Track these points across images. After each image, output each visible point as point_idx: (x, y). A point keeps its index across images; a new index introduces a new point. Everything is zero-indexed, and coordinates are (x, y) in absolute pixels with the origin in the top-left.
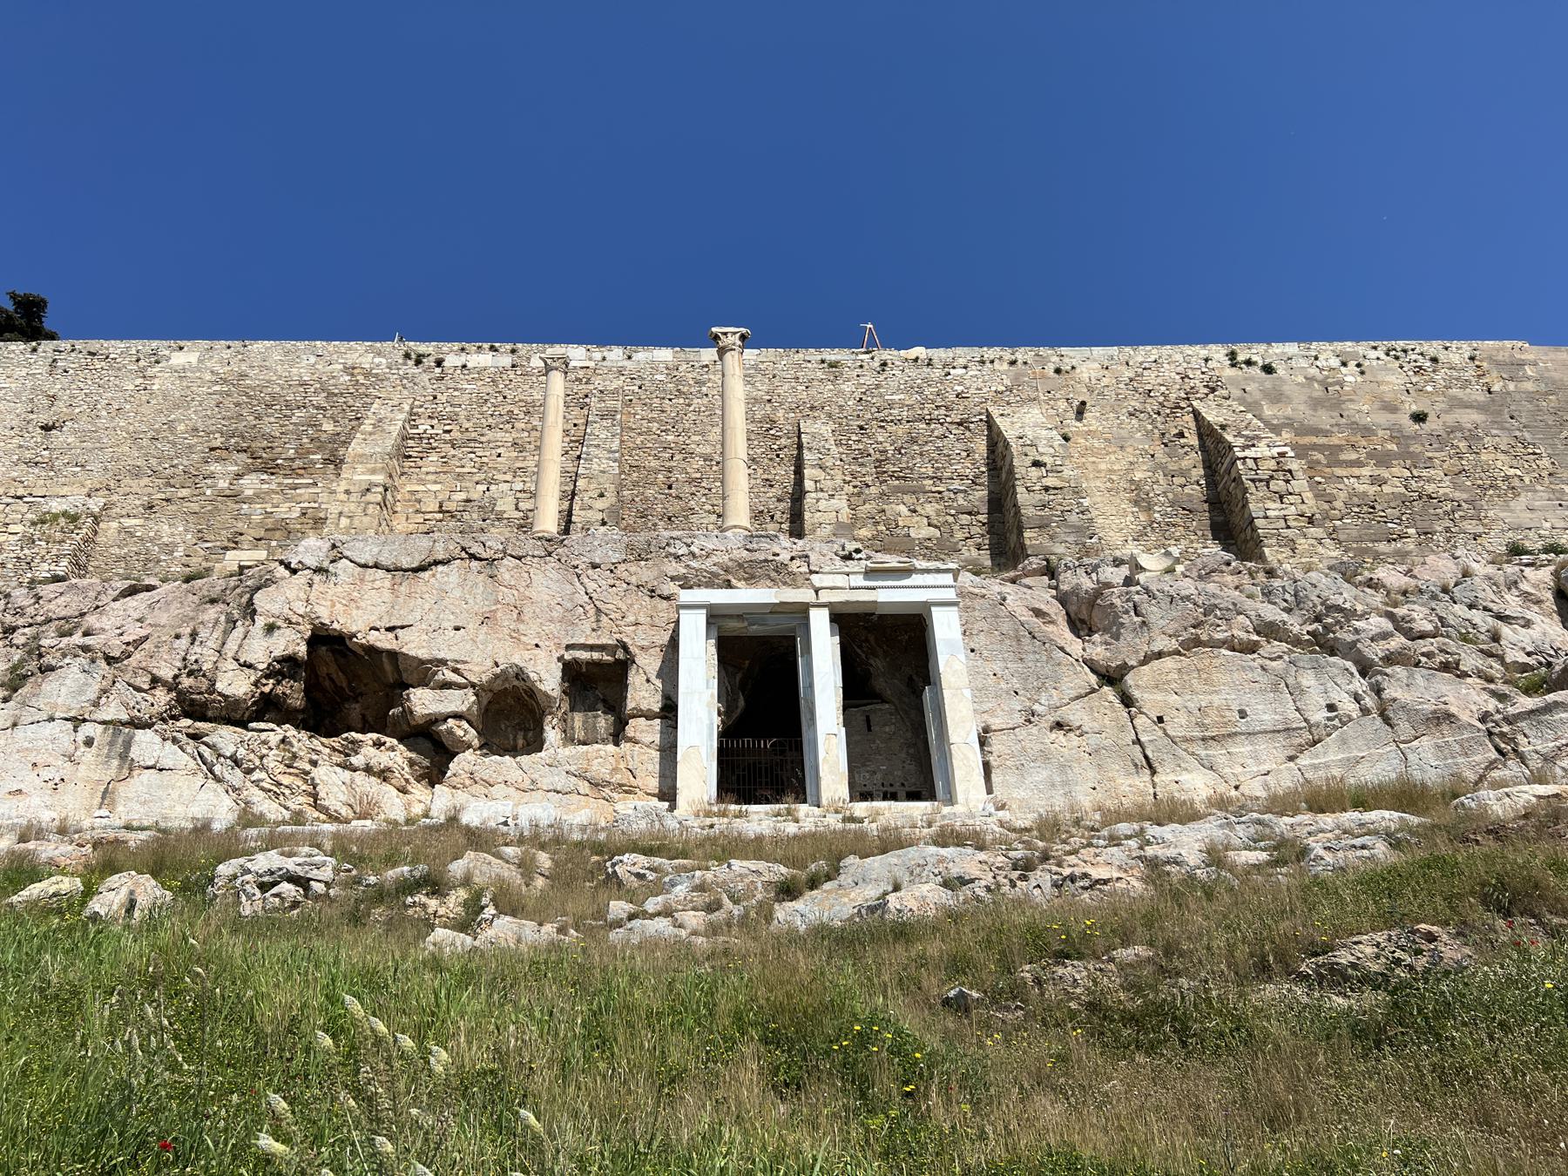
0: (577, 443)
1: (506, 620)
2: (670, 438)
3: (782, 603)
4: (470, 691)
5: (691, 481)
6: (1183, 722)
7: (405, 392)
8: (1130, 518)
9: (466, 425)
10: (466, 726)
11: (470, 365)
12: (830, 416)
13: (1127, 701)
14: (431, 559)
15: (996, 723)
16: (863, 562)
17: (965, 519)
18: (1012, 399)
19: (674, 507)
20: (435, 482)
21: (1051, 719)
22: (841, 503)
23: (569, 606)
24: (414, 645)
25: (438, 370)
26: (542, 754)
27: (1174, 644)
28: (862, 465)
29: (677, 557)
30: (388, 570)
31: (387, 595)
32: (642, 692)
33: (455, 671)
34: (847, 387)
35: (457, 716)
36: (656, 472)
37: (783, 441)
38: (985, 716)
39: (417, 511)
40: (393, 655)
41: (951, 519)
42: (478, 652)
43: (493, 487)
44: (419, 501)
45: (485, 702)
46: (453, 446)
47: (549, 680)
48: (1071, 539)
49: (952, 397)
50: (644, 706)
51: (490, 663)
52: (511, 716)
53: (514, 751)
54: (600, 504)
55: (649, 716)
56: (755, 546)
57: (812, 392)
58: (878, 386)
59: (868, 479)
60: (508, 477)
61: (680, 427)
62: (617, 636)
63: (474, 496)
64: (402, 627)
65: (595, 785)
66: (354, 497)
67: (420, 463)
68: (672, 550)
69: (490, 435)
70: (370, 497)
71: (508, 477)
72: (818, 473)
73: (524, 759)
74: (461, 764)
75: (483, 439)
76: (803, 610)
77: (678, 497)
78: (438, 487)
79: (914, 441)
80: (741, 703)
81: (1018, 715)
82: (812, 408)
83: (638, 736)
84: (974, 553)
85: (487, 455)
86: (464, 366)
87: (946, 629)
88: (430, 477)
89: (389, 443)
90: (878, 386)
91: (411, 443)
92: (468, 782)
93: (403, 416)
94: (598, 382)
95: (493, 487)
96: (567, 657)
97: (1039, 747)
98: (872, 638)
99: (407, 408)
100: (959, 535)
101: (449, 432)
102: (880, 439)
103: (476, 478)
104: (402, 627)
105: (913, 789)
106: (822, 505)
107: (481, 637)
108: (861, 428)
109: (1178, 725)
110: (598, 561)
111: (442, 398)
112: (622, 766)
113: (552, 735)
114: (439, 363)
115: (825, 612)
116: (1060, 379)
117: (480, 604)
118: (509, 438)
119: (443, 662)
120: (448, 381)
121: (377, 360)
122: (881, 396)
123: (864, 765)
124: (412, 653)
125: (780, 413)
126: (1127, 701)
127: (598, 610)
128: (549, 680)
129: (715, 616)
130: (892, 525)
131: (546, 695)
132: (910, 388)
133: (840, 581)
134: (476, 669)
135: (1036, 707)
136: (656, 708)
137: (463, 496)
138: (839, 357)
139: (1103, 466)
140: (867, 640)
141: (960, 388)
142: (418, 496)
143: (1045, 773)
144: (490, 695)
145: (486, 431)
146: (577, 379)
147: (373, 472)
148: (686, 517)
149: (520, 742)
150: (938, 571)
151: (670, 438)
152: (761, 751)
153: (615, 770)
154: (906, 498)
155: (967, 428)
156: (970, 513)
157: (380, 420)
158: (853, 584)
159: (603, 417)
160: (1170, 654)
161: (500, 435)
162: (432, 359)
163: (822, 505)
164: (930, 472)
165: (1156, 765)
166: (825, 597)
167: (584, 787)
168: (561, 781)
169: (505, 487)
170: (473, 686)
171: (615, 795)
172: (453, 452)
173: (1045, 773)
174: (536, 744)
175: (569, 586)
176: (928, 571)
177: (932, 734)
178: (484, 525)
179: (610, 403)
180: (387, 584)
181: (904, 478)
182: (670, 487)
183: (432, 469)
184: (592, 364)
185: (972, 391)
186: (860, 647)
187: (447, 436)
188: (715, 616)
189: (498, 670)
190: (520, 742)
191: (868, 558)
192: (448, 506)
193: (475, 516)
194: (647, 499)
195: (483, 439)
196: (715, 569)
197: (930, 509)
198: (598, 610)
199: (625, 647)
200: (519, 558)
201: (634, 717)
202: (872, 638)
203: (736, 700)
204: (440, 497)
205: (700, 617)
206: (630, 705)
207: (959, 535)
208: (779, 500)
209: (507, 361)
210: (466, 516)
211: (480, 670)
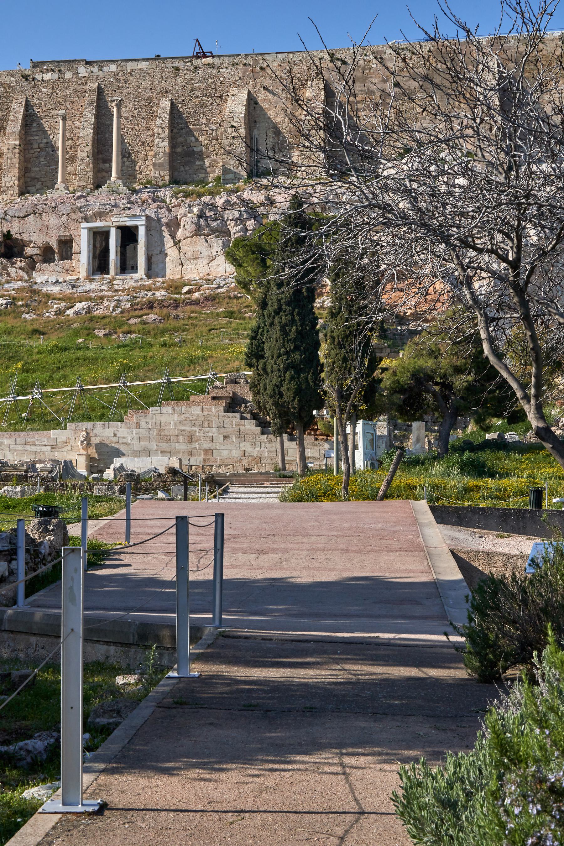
1: (45, 230)
13: (180, 249)
24: (25, 237)
47: (54, 245)
52: (47, 254)
54: (87, 149)
65: (67, 270)
66: (10, 151)
88: (35, 133)
90: (192, 79)
102: (189, 106)
108: (183, 101)
109: (189, 255)
117: (38, 225)
119: (32, 242)
126: (180, 249)
128: (54, 245)
129: (90, 229)
132: (205, 79)
138: (179, 65)
146: (82, 83)
152: (100, 265)
167: (64, 271)
168: (59, 270)
184: (86, 75)
207: (211, 149)
209: (56, 76)
211: (39, 243)
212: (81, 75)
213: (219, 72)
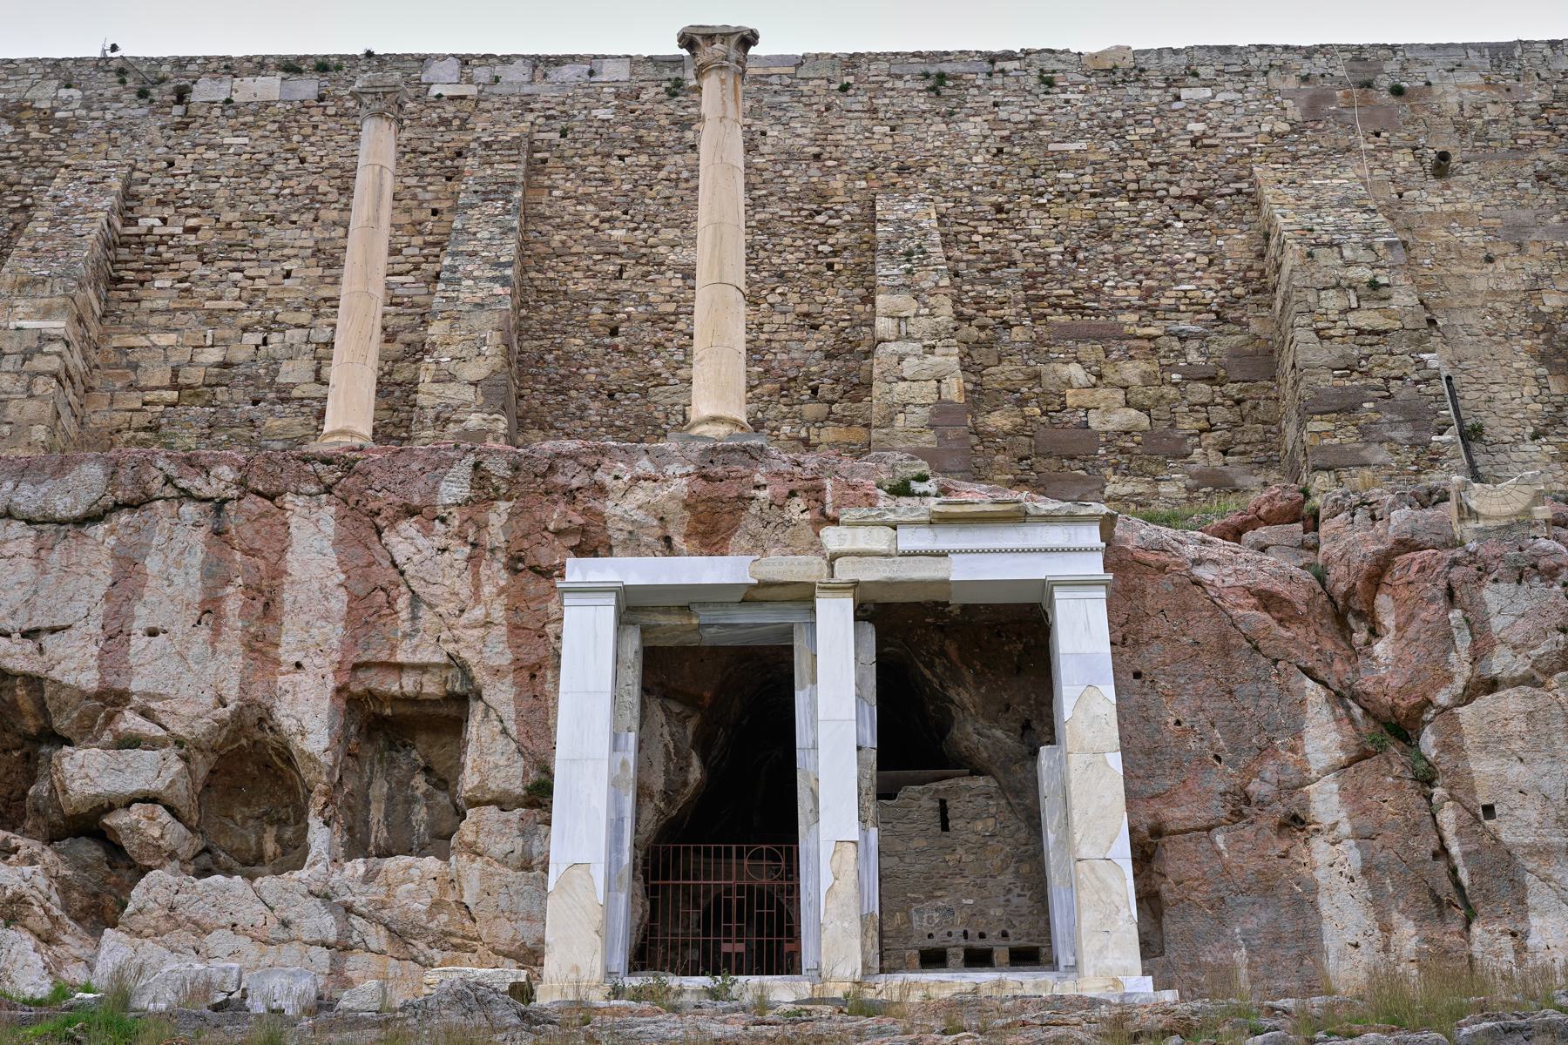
0: (425, 247)
2: (618, 234)
3: (765, 584)
4: (172, 753)
5: (657, 319)
6: (1533, 816)
7: (116, 154)
8: (1530, 389)
9: (228, 216)
10: (165, 817)
11: (236, 98)
12: (936, 184)
14: (109, 500)
15: (1175, 815)
16: (932, 503)
17: (1201, 391)
18: (1303, 150)
19: (620, 371)
20: (167, 329)
21: (1280, 809)
22: (948, 359)
23: (360, 589)
25: (178, 110)
26: (303, 874)
27: (1521, 667)
28: (998, 283)
29: (571, 495)
30: (29, 522)
31: (26, 568)
32: (487, 758)
33: (146, 713)
34: (973, 128)
35: (149, 799)
36: (586, 300)
37: (841, 237)
38: (1156, 805)
39: (131, 387)
40: (34, 682)
41: (1172, 392)
42: (188, 678)
43: (275, 338)
44: (135, 367)
45: (202, 772)
46: (201, 259)
48: (1402, 434)
49: (1183, 146)
50: (495, 785)
51: (209, 699)
53: (250, 863)
55: (502, 802)
56: (719, 470)
57: (904, 137)
58: (1035, 125)
59: (1008, 312)
60: (304, 317)
61: (637, 211)
62: (451, 648)
63: (240, 354)
64: (53, 630)
67: (140, 293)
68: (559, 479)
69: (272, 233)
70: (39, 363)
71: (304, 317)
72: (905, 303)
73: (267, 882)
74: (153, 890)
75: (260, 243)
76: (803, 596)
77: (628, 351)
78: (170, 339)
79: (1104, 234)
80: (695, 773)
81: (1216, 802)
82: (902, 170)
83: (483, 842)
84: (1216, 460)
85: (264, 275)
86: (228, 101)
87: (1082, 635)
88: (157, 320)
89: (85, 253)
91: (124, 253)
92: (163, 925)
93: (109, 201)
94: (480, 126)
95: (275, 338)
96: (356, 688)
97: (1253, 865)
98: (952, 649)
99: (116, 184)
100: (1188, 425)
101: (194, 230)
102: (1036, 230)
103: (244, 319)
104: (53, 630)
105: (1024, 942)
106: (910, 367)
107: (196, 650)
108: (999, 209)
110: (417, 500)
111: (184, 164)
112: (451, 897)
113: (319, 837)
114: (181, 95)
115: (847, 604)
116: (1402, 109)
118: (306, 240)
120: (196, 132)
121: (63, 93)
122: (1041, 142)
123: (930, 897)
124: (69, 679)
125: (837, 183)
127: (415, 598)
129: (633, 607)
130: (1054, 403)
131: (311, 758)
133: (878, 539)
134: (185, 710)
135: (1255, 787)
136: (517, 788)
137: (214, 355)
139: (1480, 284)
140: (943, 653)
141: (1197, 127)
142: (133, 357)
143: (1264, 916)
144: (213, 758)
145: (264, 227)
147: (47, 313)
148: (644, 392)
149: (270, 847)
150: (1072, 519)
151: (618, 234)
153: (437, 906)
154: (1084, 350)
155: (1210, 208)
156: (1211, 380)
157: (65, 212)
158: (904, 545)
159: (486, 197)
160: (1515, 683)
161: (289, 234)
162: (167, 87)
163: (910, 367)
164: (1134, 296)
165: (1475, 900)
166: (846, 572)
169: (296, 336)
170: (179, 743)
171: (436, 954)
172: (201, 270)
173: (1264, 916)
174: (293, 854)
175: (360, 550)
176: (1049, 519)
177: (1051, 836)
178: (255, 412)
179: (503, 169)
180: (28, 547)
181: (1081, 309)
182: (614, 332)
183: (160, 304)
184: (470, 90)
185: (1224, 132)
186: (930, 666)
187: (191, 239)
188: (633, 607)
189: (224, 713)
190: (270, 847)
191: (944, 491)
192: (194, 376)
193: (238, 394)
194: (568, 358)
195: (260, 243)
196: (639, 515)
197: (1131, 371)
198: (415, 598)
199: (464, 668)
200: (271, 498)
201: (477, 803)
202: (952, 649)
203: (684, 769)
204: (175, 358)
205: (606, 614)
206: (469, 781)
207: (1188, 425)
208: (829, 356)
210: (222, 394)
212: (435, 90)
213: (1178, 98)
